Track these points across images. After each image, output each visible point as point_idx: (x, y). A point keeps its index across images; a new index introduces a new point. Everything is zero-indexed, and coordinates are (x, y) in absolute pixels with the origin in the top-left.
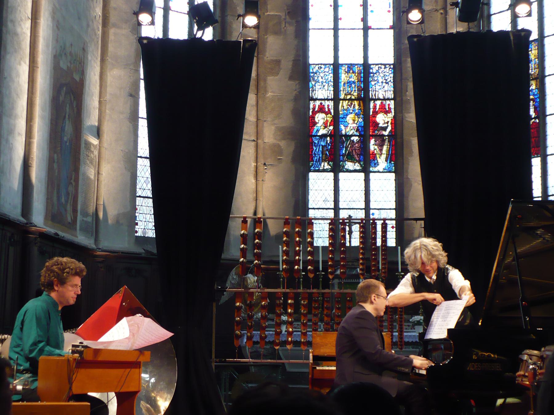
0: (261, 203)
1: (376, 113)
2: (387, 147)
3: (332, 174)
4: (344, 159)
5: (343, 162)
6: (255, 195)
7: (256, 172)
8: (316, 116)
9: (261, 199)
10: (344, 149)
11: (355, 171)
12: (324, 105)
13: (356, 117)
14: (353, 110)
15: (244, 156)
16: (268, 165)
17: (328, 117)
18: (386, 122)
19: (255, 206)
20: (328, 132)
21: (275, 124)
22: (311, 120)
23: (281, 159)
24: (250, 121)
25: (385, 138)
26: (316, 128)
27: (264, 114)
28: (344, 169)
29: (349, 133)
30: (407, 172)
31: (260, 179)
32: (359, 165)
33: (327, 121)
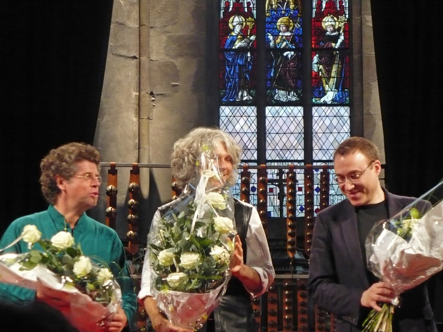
0: (146, 153)
1: (321, 15)
2: (338, 67)
3: (254, 108)
4: (272, 86)
5: (270, 89)
6: (137, 141)
7: (139, 105)
8: (231, 20)
9: (146, 147)
10: (273, 70)
11: (290, 104)
12: (242, 3)
13: (291, 21)
14: (285, 11)
15: (119, 82)
16: (157, 95)
17: (248, 22)
18: (337, 27)
19: (137, 158)
20: (249, 44)
21: (168, 32)
22: (223, 26)
23: (176, 85)
24: (129, 28)
25: (335, 53)
26: (229, 39)
27: (151, 17)
28: (273, 101)
29: (280, 45)
30: (368, 105)
31: (144, 116)
32: (295, 94)
33: (247, 27)
